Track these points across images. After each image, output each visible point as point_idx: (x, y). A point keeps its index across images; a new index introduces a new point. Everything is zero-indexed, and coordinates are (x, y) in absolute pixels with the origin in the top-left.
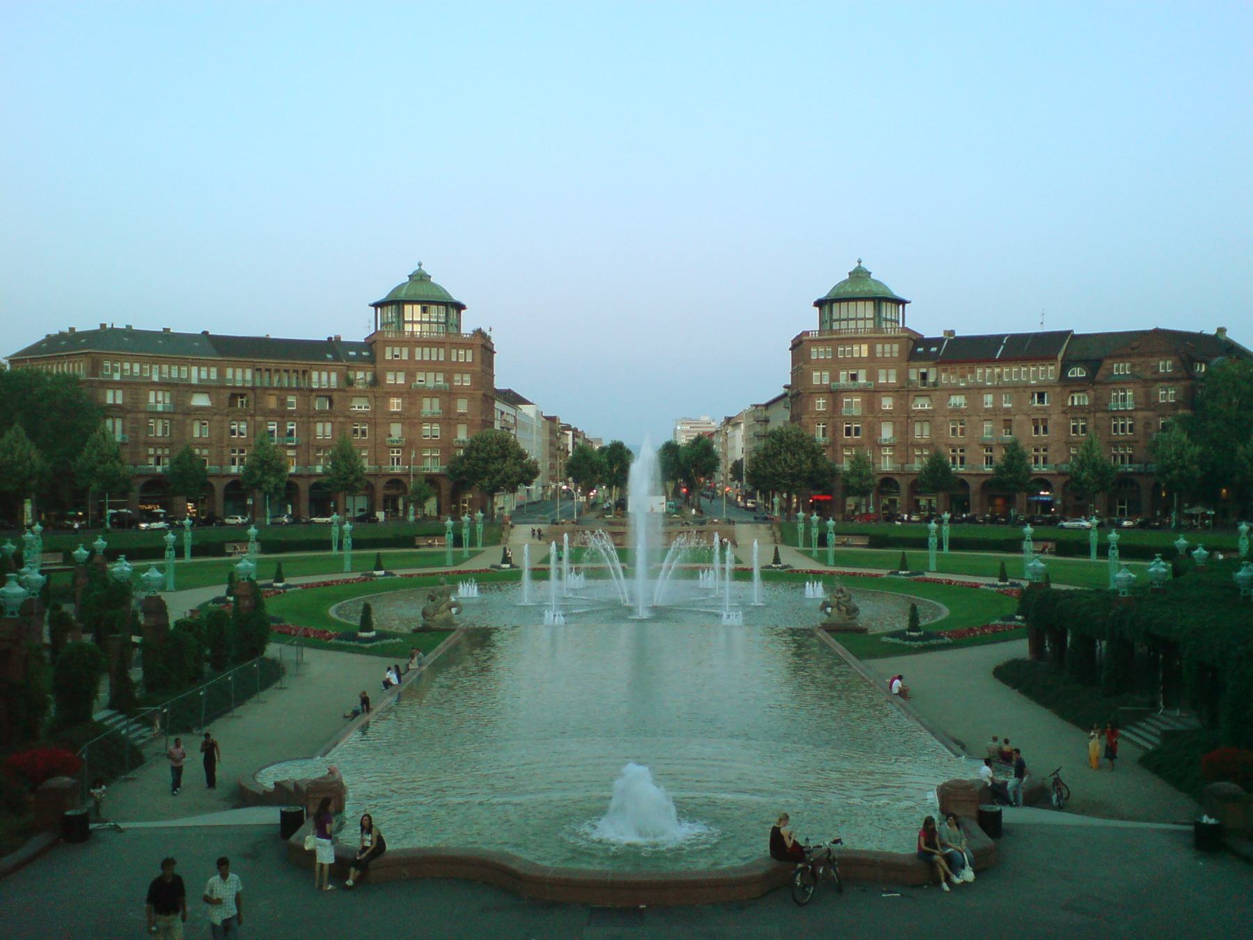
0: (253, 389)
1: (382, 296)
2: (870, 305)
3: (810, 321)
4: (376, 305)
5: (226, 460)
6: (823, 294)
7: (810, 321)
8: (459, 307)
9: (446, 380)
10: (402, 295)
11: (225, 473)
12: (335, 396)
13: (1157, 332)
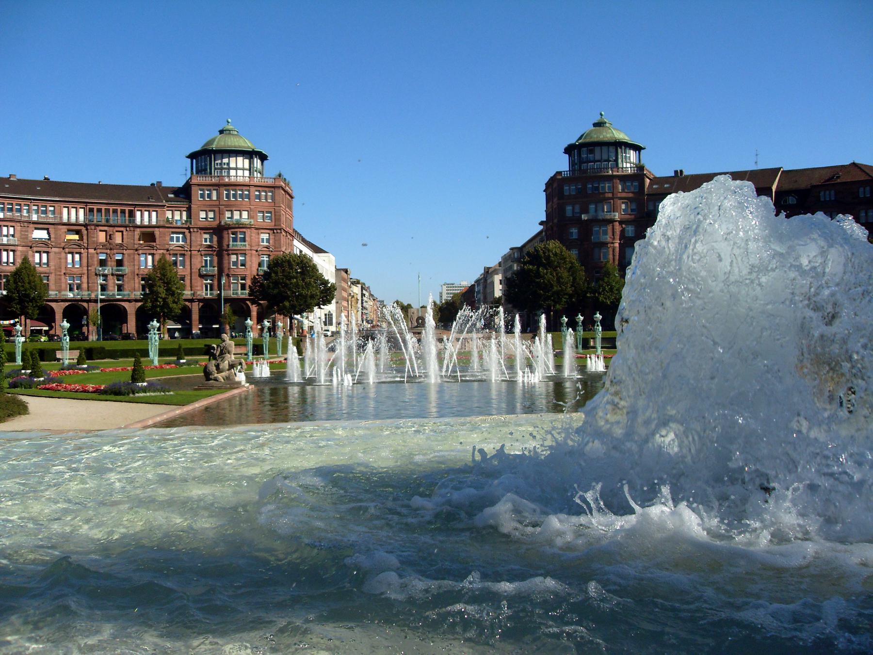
0: (85, 226)
1: (197, 148)
2: (612, 149)
3: (563, 164)
4: (192, 156)
5: (63, 285)
6: (573, 141)
7: (563, 164)
8: (263, 158)
9: (249, 217)
10: (214, 147)
11: (63, 298)
12: (157, 232)
13: (854, 164)
